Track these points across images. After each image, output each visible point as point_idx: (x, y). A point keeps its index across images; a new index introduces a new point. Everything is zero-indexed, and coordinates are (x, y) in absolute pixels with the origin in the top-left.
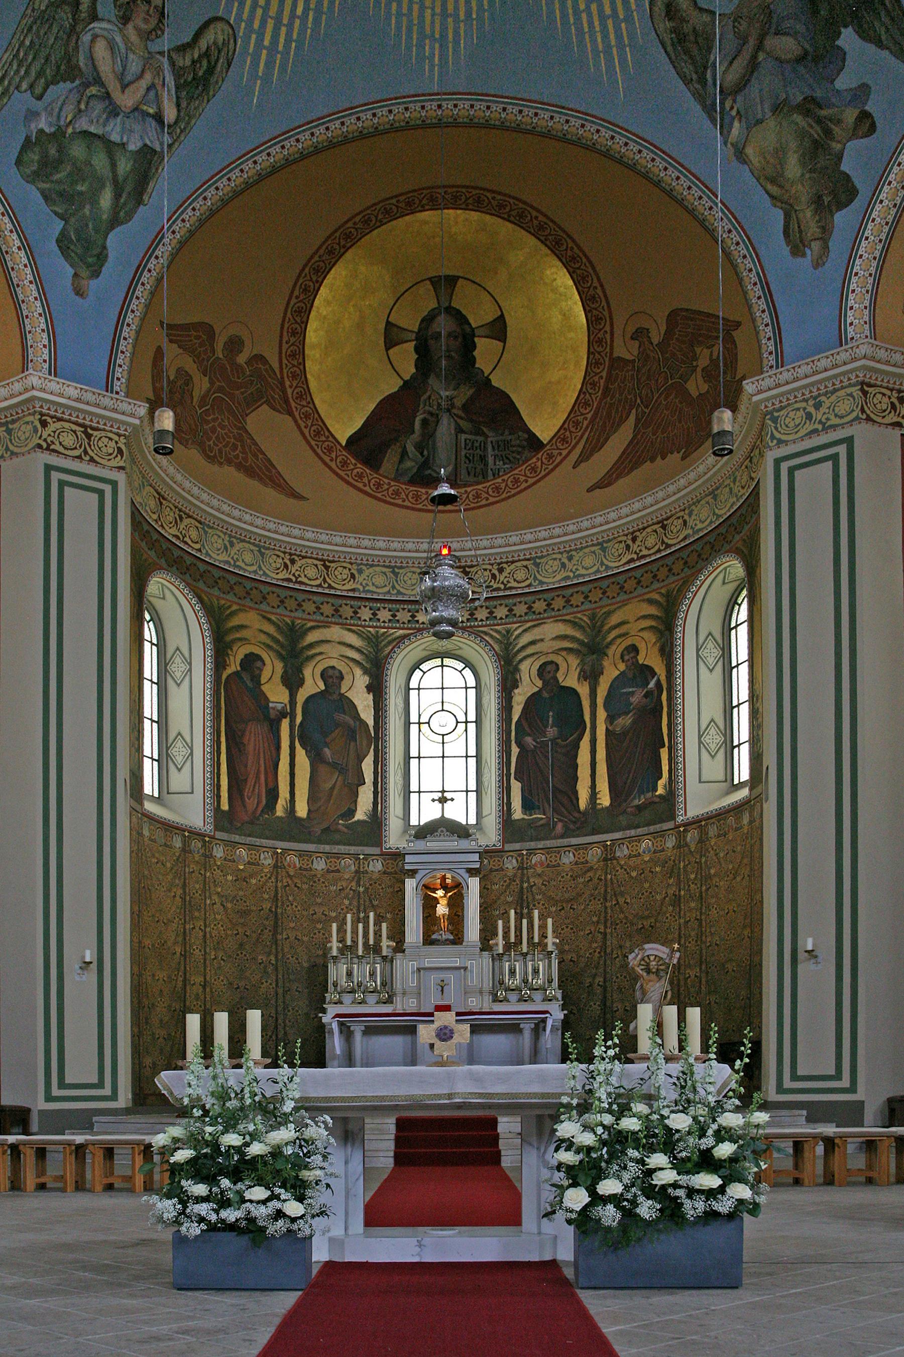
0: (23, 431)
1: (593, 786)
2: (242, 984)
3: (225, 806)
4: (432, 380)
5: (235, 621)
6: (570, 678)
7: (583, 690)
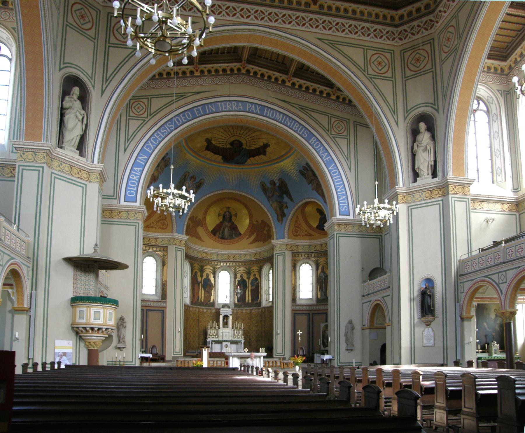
6: (245, 278)
7: (247, 281)
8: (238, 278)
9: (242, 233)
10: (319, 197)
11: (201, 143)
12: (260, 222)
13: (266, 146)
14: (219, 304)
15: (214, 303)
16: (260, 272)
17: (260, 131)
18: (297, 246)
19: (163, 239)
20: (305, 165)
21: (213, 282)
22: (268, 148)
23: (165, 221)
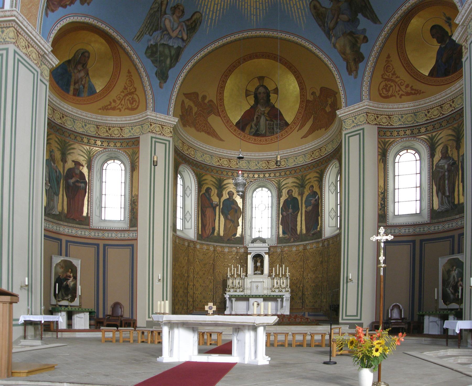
0: (146, 127)
1: (301, 227)
2: (204, 285)
3: (200, 233)
4: (259, 106)
5: (204, 178)
7: (299, 198)
8: (284, 197)
16: (320, 180)
18: (389, 117)
19: (132, 126)
21: (240, 205)
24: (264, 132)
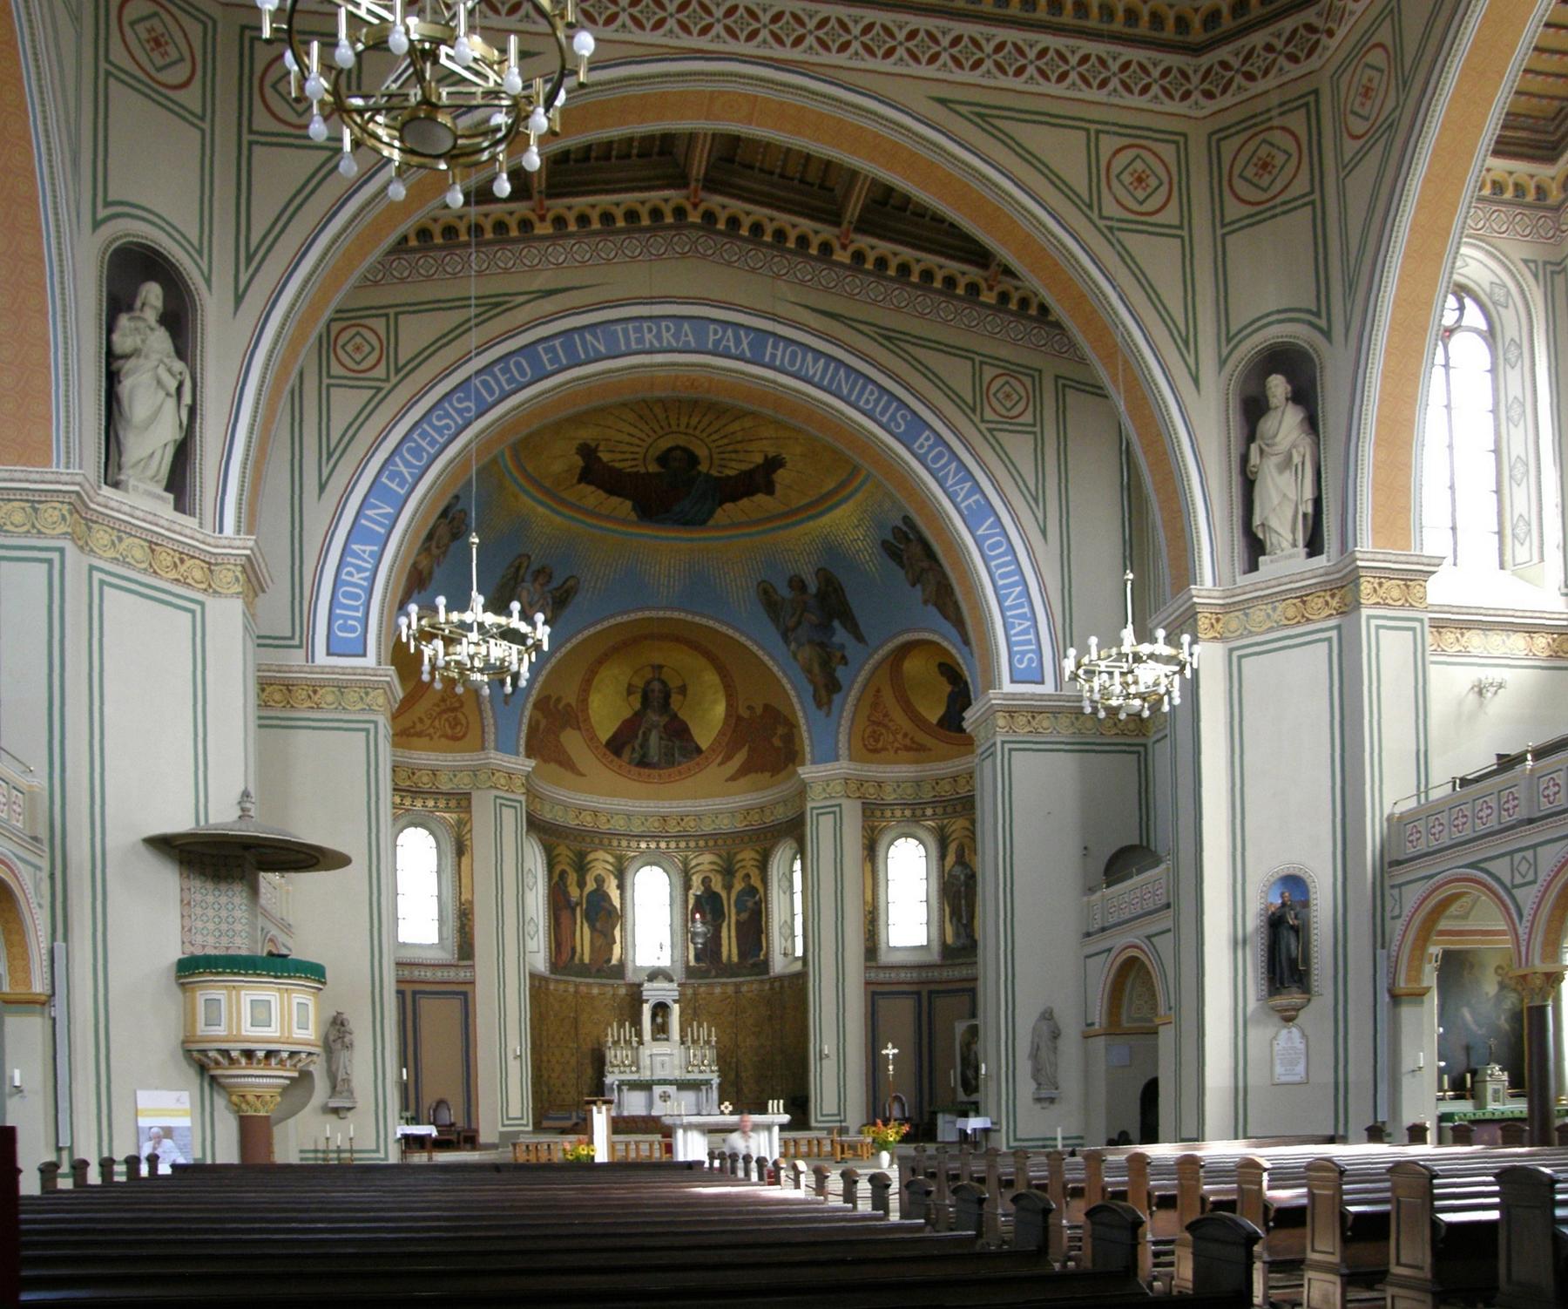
6: (717, 885)
7: (724, 895)
8: (697, 889)
9: (704, 746)
10: (947, 627)
11: (562, 459)
12: (759, 711)
13: (773, 464)
14: (637, 970)
15: (622, 965)
16: (763, 866)
17: (753, 414)
18: (880, 784)
19: (455, 771)
20: (900, 524)
21: (617, 903)
22: (780, 471)
23: (460, 716)
24: (656, 759)
